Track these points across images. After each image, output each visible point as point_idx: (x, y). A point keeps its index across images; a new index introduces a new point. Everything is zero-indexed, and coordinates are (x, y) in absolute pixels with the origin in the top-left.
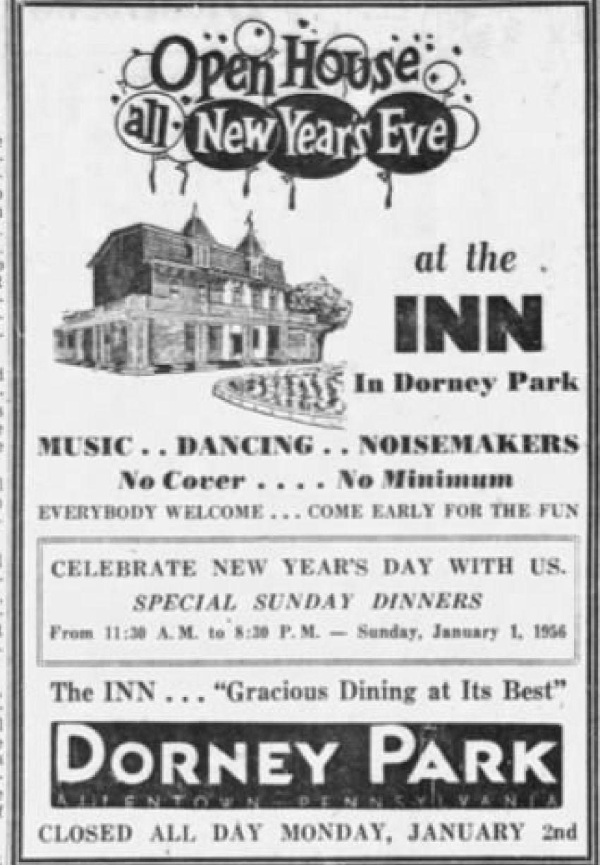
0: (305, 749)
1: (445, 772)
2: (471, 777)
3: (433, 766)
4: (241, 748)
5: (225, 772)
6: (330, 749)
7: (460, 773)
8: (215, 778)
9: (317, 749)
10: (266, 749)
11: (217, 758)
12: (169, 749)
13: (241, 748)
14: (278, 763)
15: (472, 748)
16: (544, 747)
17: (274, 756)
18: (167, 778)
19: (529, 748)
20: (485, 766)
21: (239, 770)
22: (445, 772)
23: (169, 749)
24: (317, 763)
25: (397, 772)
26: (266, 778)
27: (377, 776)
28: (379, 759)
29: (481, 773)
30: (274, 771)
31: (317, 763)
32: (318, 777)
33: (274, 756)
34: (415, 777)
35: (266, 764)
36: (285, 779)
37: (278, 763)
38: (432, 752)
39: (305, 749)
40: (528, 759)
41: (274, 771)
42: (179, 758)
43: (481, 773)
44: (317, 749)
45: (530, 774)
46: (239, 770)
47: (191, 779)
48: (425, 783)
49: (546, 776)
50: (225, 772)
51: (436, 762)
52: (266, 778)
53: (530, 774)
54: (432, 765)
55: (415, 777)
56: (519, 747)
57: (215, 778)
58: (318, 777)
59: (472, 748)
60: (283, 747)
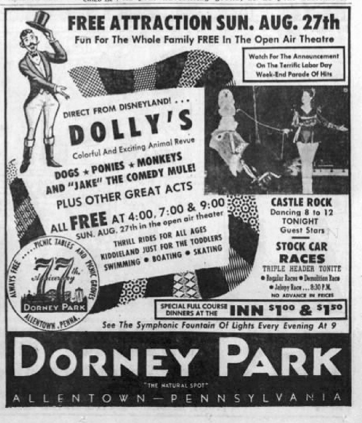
0: (176, 353)
1: (269, 369)
2: (285, 372)
3: (261, 365)
4: (134, 353)
5: (123, 368)
6: (193, 353)
7: (278, 367)
8: (117, 372)
9: (184, 354)
10: (151, 353)
11: (119, 359)
12: (87, 353)
13: (134, 353)
14: (159, 363)
15: (287, 352)
16: (334, 352)
17: (156, 358)
18: (86, 372)
19: (322, 354)
20: (295, 365)
21: (133, 366)
22: (269, 369)
23: (87, 353)
24: (185, 362)
25: (236, 369)
26: (151, 372)
27: (223, 372)
28: (225, 360)
29: (292, 370)
30: (156, 368)
31: (185, 362)
32: (185, 372)
33: (156, 358)
34: (248, 373)
35: (151, 362)
36: (163, 373)
37: (159, 363)
38: (260, 355)
39: (176, 353)
40: (324, 360)
41: (156, 368)
42: (94, 359)
43: (292, 370)
44: (184, 354)
45: (323, 367)
46: (133, 366)
47: (102, 373)
48: (254, 374)
49: (334, 371)
50: (123, 368)
51: (263, 363)
52: (151, 372)
53: (323, 367)
54: (260, 364)
55: (248, 373)
56: (317, 351)
57: (117, 372)
58: (185, 372)
59: (287, 352)
60: (162, 352)
